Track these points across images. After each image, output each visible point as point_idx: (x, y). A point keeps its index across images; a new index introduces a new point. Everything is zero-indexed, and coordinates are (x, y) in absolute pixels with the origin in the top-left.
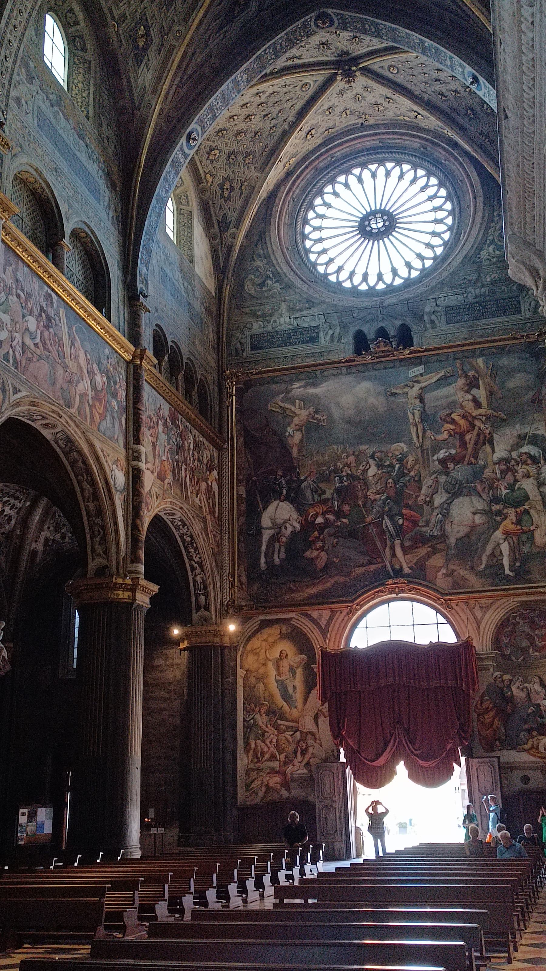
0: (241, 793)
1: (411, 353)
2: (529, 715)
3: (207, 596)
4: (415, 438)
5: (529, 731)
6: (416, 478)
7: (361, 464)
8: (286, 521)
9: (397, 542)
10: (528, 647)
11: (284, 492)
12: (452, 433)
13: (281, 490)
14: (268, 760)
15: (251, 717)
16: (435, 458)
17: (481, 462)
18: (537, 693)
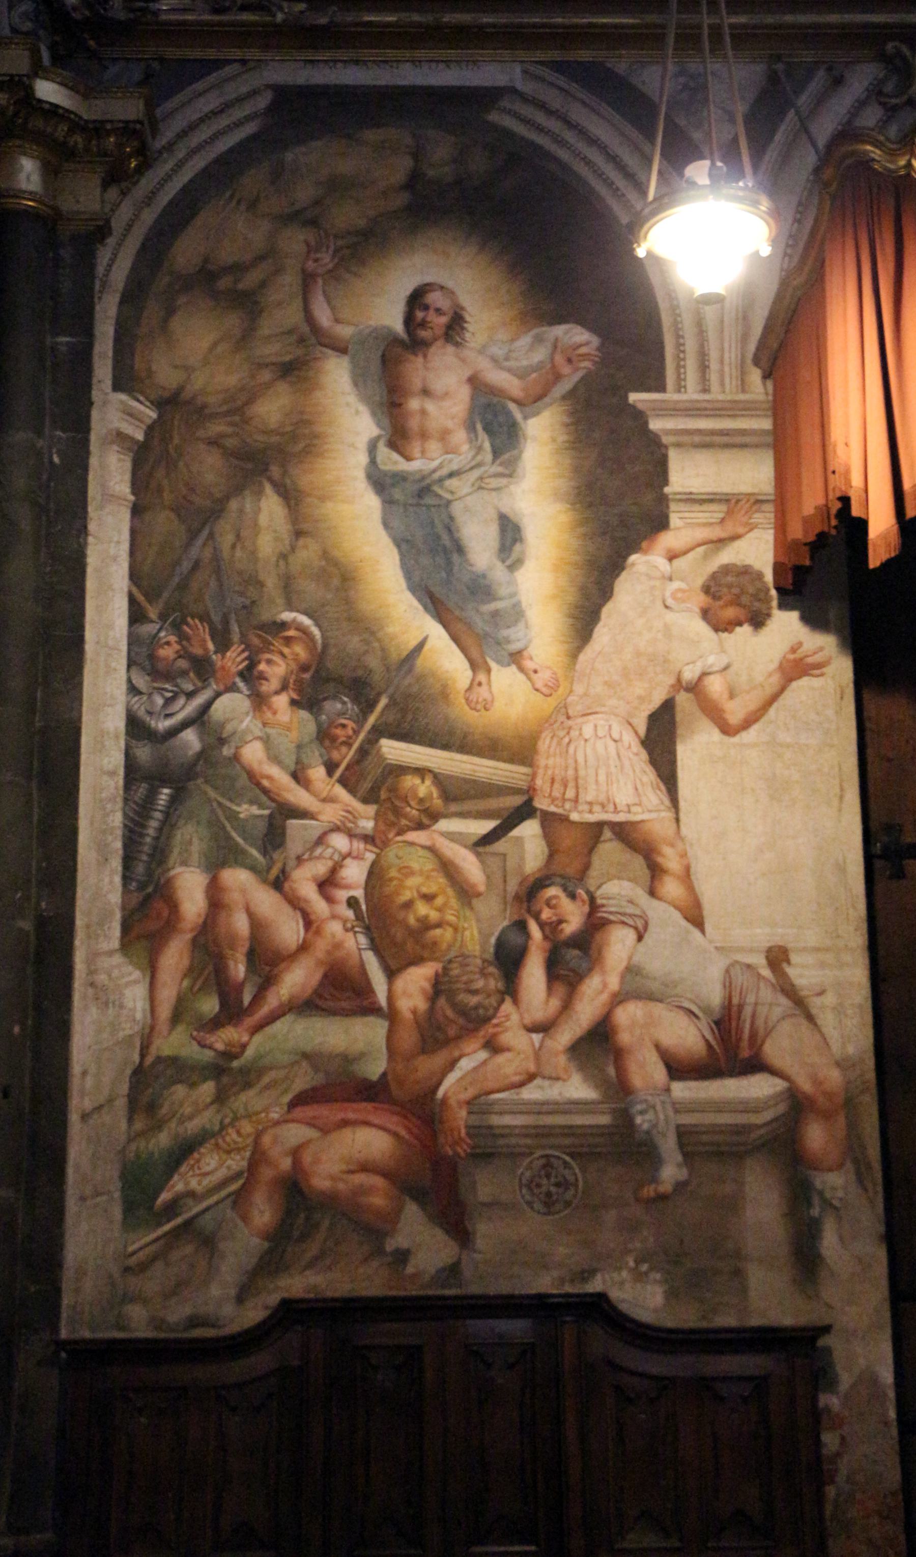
0: (92, 1236)
14: (308, 1005)
15: (186, 709)
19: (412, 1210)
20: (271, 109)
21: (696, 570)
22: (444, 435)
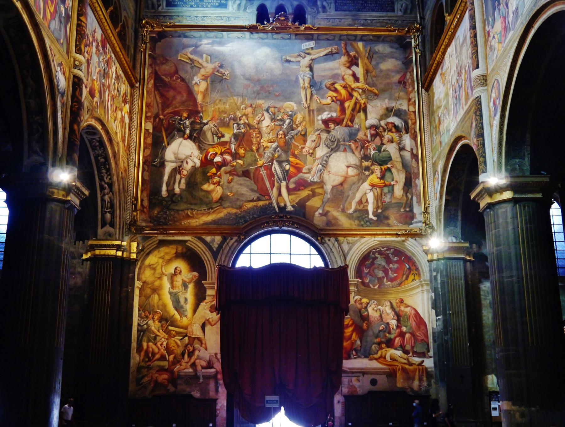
0: (132, 387)
1: (306, 29)
2: (380, 331)
3: (113, 214)
4: (304, 100)
5: (379, 344)
6: (303, 133)
7: (257, 115)
8: (187, 157)
9: (284, 184)
10: (383, 277)
11: (188, 131)
12: (335, 99)
13: (185, 130)
16: (319, 118)
17: (356, 126)
18: (388, 314)
19: (170, 385)
20: (158, 243)
21: (209, 305)
22: (178, 287)
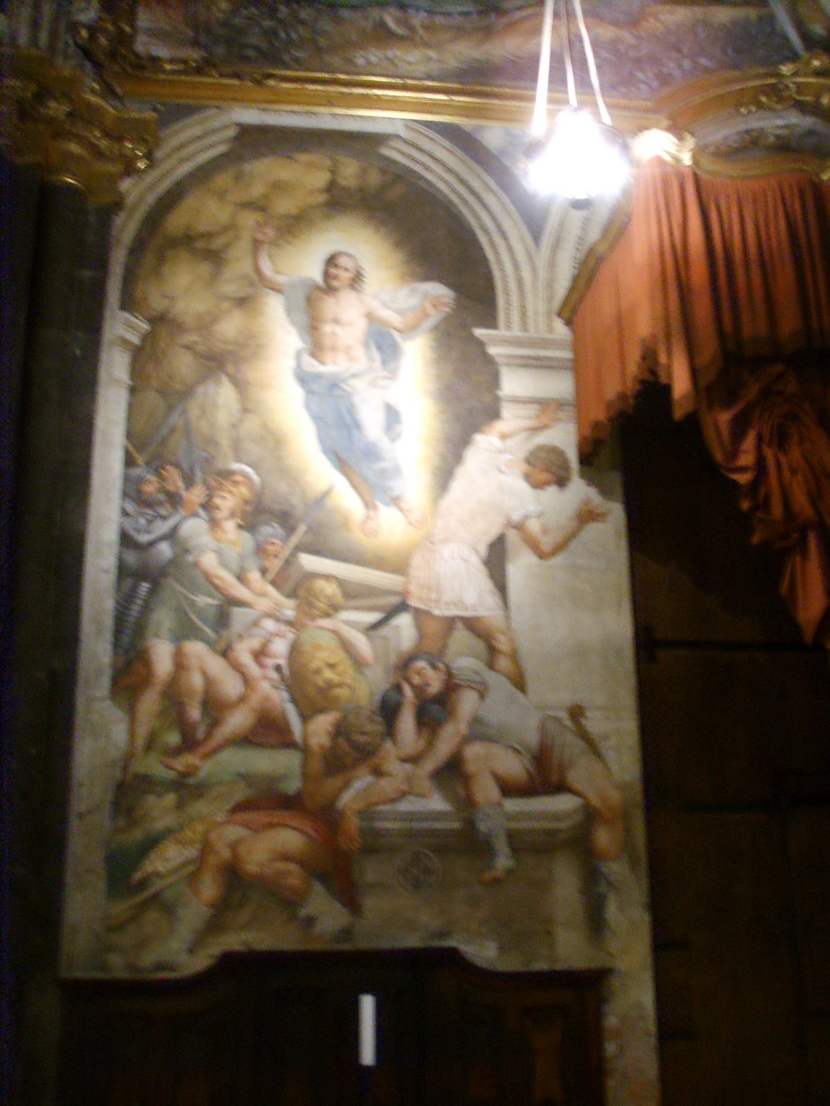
0: (85, 905)
14: (246, 740)
15: (162, 527)
19: (318, 889)
22: (348, 350)
